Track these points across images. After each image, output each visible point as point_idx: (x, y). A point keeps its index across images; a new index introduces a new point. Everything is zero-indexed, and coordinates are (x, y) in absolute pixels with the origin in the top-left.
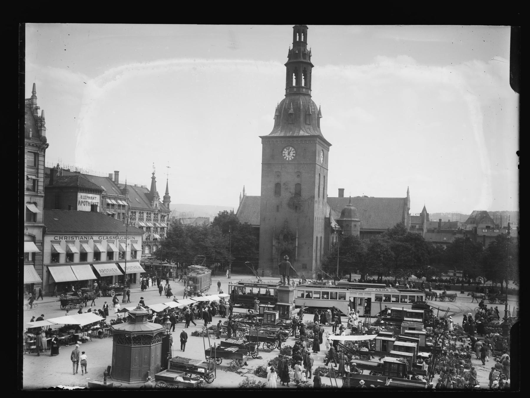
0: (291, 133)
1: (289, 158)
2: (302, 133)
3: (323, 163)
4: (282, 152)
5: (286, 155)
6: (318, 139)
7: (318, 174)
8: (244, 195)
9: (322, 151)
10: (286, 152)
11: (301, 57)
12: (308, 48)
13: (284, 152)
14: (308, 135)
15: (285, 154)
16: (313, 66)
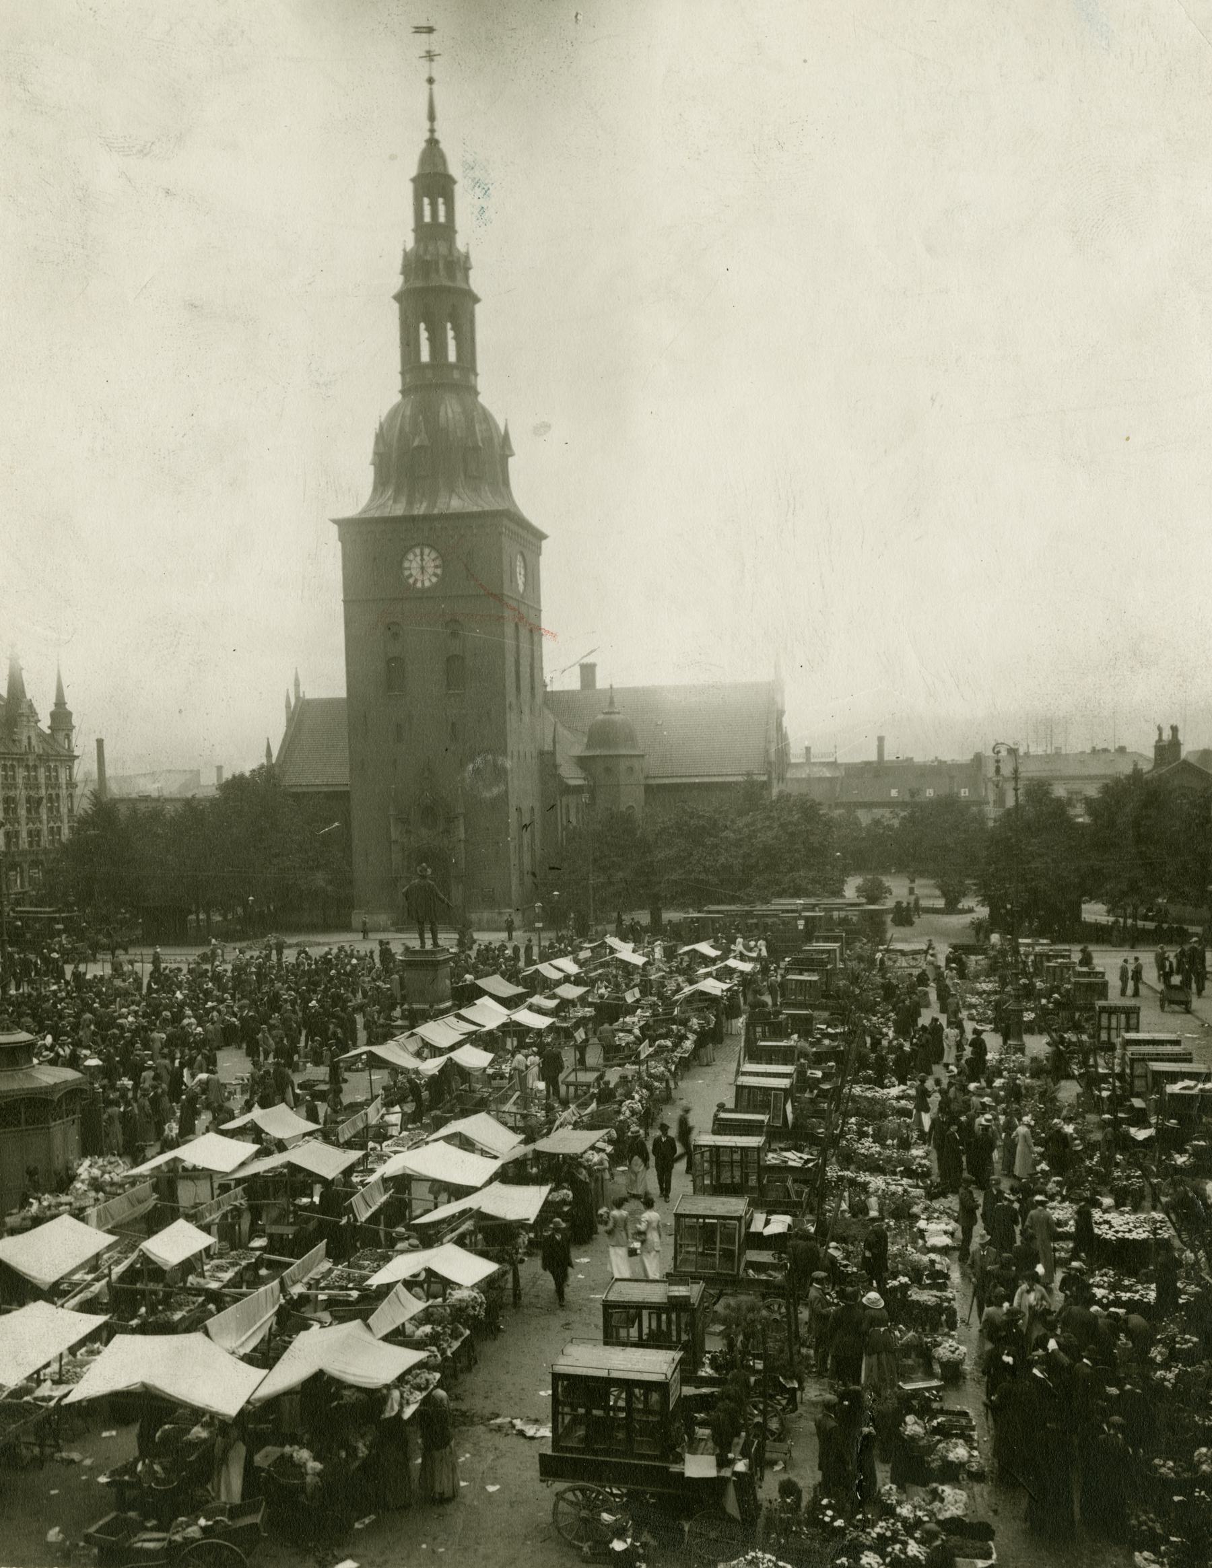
0: (425, 505)
1: (423, 582)
2: (456, 504)
3: (525, 590)
4: (401, 563)
5: (414, 572)
6: (506, 522)
7: (513, 625)
8: (298, 698)
9: (519, 558)
10: (413, 564)
11: (442, 272)
12: (461, 244)
13: (406, 564)
14: (475, 509)
15: (409, 569)
16: (476, 300)
